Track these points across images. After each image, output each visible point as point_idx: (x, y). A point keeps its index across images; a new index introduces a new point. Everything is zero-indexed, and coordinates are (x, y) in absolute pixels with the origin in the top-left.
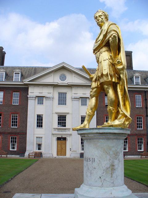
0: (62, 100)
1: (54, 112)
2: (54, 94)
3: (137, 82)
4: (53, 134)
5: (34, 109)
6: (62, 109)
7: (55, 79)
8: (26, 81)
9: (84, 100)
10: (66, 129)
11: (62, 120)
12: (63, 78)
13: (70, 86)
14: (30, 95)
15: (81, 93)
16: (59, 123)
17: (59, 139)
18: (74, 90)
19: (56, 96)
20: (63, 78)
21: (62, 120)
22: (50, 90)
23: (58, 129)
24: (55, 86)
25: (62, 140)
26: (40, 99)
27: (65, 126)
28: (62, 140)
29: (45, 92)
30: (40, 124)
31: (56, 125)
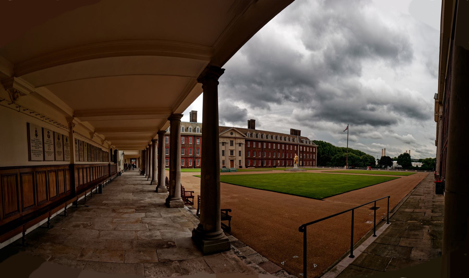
0: (232, 144)
2: (228, 141)
3: (315, 157)
6: (232, 148)
7: (229, 135)
9: (240, 144)
11: (232, 152)
12: (232, 134)
15: (239, 141)
17: (231, 161)
19: (229, 142)
20: (232, 134)
21: (232, 152)
25: (232, 161)
26: (223, 144)
28: (232, 161)
29: (225, 140)
30: (223, 155)
31: (229, 155)
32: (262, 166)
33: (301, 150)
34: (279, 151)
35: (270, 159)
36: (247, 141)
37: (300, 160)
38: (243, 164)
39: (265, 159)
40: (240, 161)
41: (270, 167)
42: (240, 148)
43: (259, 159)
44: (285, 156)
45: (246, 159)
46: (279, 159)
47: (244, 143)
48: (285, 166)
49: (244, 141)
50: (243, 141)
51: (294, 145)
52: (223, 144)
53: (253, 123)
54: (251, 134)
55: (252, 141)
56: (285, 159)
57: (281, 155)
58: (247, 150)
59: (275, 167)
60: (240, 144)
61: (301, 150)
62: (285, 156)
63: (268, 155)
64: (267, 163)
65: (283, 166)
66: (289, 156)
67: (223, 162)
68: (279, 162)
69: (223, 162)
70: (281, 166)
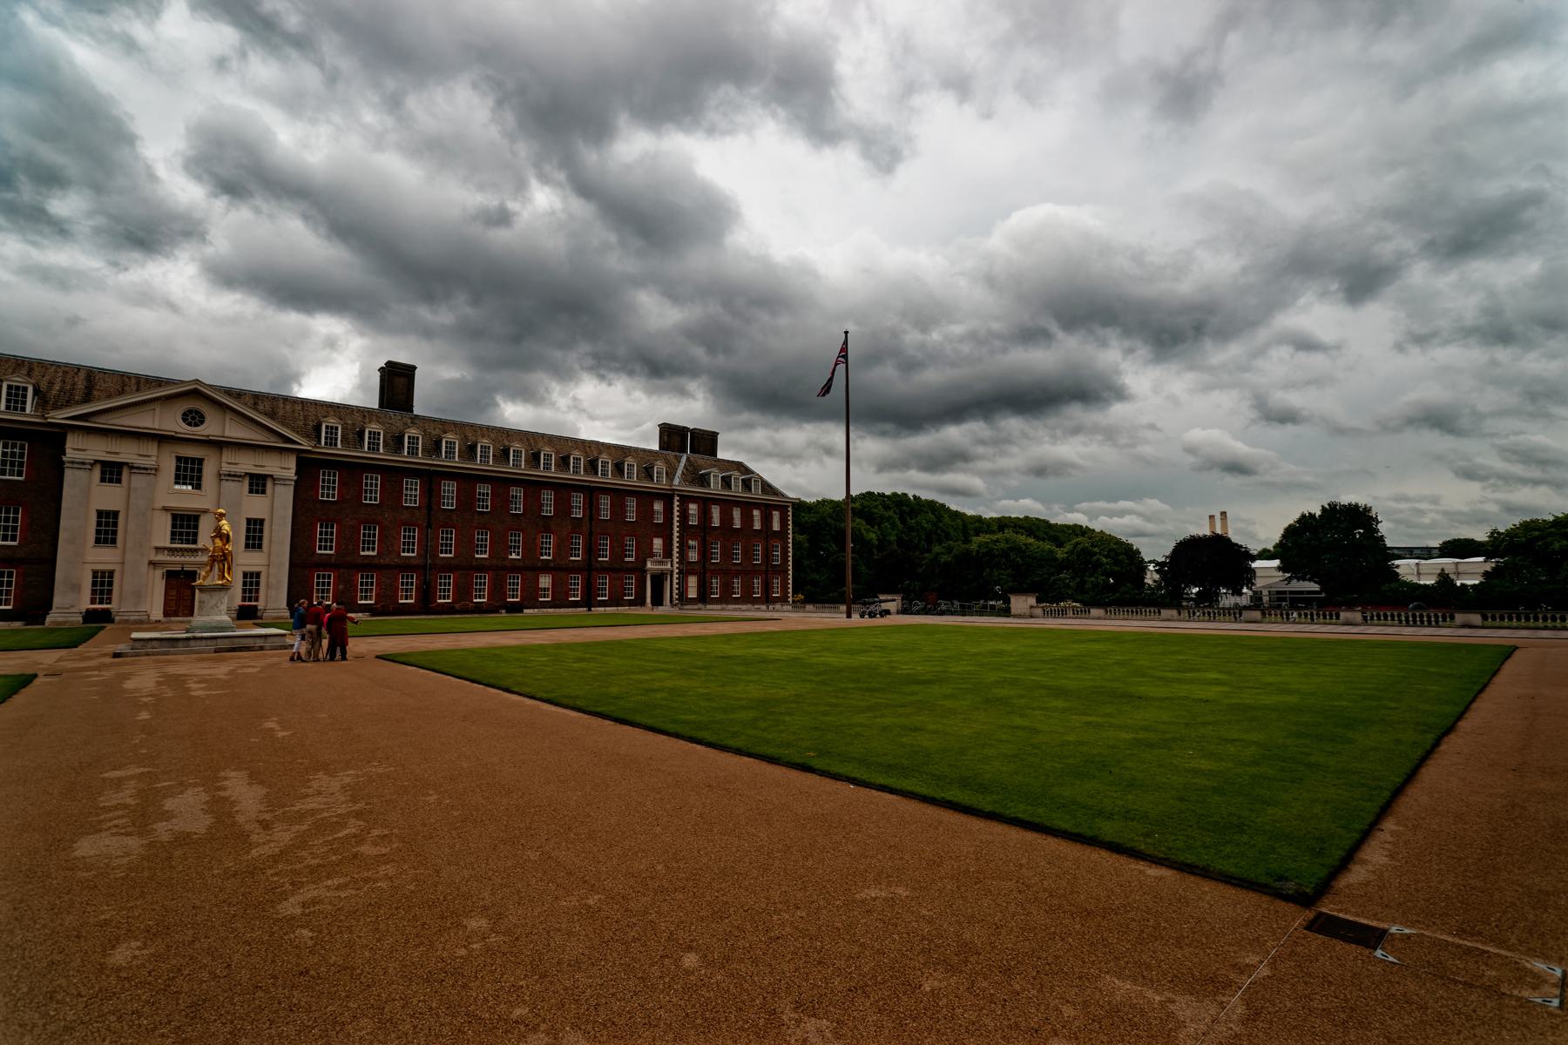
1: (159, 505)
4: (153, 564)
5: (83, 497)
6: (185, 497)
7: (170, 421)
8: (59, 416)
9: (258, 483)
10: (196, 550)
11: (185, 525)
12: (194, 418)
13: (219, 445)
14: (70, 455)
15: (247, 463)
16: (173, 534)
17: (170, 575)
18: (228, 456)
19: (169, 466)
20: (194, 418)
21: (185, 525)
22: (152, 449)
23: (171, 550)
24: (162, 439)
27: (195, 542)
29: (127, 452)
32: (426, 605)
33: (693, 522)
34: (546, 525)
35: (481, 567)
36: (308, 467)
37: (684, 574)
38: (274, 597)
39: (448, 567)
40: (252, 581)
41: (479, 609)
42: (256, 506)
43: (407, 567)
44: (591, 551)
45: (302, 565)
46: (546, 568)
47: (291, 474)
48: (588, 601)
49: (291, 463)
50: (285, 468)
51: (646, 498)
52: (112, 472)
53: (400, 381)
54: (396, 442)
55: (352, 471)
56: (589, 569)
57: (564, 548)
58: (306, 512)
59: (516, 608)
60: (258, 483)
61: (693, 522)
62: (591, 551)
63: (500, 547)
64: (463, 592)
65: (575, 605)
66: (619, 551)
67: (103, 583)
68: (545, 581)
69: (103, 583)
70: (560, 601)
